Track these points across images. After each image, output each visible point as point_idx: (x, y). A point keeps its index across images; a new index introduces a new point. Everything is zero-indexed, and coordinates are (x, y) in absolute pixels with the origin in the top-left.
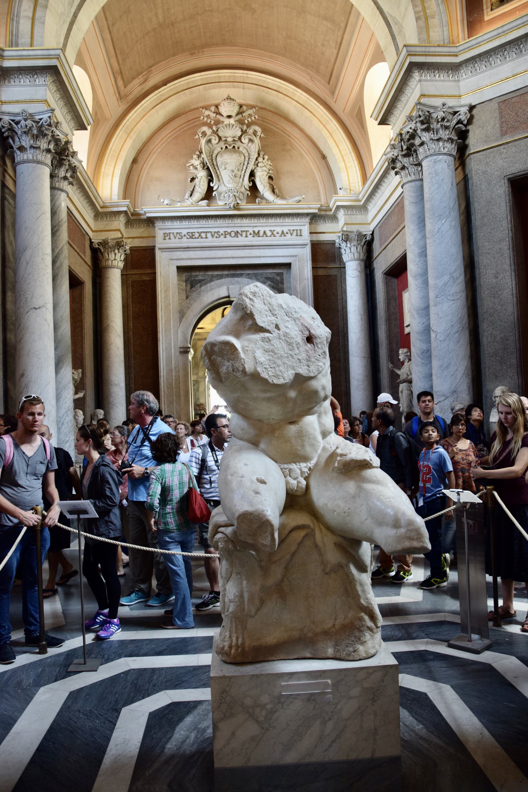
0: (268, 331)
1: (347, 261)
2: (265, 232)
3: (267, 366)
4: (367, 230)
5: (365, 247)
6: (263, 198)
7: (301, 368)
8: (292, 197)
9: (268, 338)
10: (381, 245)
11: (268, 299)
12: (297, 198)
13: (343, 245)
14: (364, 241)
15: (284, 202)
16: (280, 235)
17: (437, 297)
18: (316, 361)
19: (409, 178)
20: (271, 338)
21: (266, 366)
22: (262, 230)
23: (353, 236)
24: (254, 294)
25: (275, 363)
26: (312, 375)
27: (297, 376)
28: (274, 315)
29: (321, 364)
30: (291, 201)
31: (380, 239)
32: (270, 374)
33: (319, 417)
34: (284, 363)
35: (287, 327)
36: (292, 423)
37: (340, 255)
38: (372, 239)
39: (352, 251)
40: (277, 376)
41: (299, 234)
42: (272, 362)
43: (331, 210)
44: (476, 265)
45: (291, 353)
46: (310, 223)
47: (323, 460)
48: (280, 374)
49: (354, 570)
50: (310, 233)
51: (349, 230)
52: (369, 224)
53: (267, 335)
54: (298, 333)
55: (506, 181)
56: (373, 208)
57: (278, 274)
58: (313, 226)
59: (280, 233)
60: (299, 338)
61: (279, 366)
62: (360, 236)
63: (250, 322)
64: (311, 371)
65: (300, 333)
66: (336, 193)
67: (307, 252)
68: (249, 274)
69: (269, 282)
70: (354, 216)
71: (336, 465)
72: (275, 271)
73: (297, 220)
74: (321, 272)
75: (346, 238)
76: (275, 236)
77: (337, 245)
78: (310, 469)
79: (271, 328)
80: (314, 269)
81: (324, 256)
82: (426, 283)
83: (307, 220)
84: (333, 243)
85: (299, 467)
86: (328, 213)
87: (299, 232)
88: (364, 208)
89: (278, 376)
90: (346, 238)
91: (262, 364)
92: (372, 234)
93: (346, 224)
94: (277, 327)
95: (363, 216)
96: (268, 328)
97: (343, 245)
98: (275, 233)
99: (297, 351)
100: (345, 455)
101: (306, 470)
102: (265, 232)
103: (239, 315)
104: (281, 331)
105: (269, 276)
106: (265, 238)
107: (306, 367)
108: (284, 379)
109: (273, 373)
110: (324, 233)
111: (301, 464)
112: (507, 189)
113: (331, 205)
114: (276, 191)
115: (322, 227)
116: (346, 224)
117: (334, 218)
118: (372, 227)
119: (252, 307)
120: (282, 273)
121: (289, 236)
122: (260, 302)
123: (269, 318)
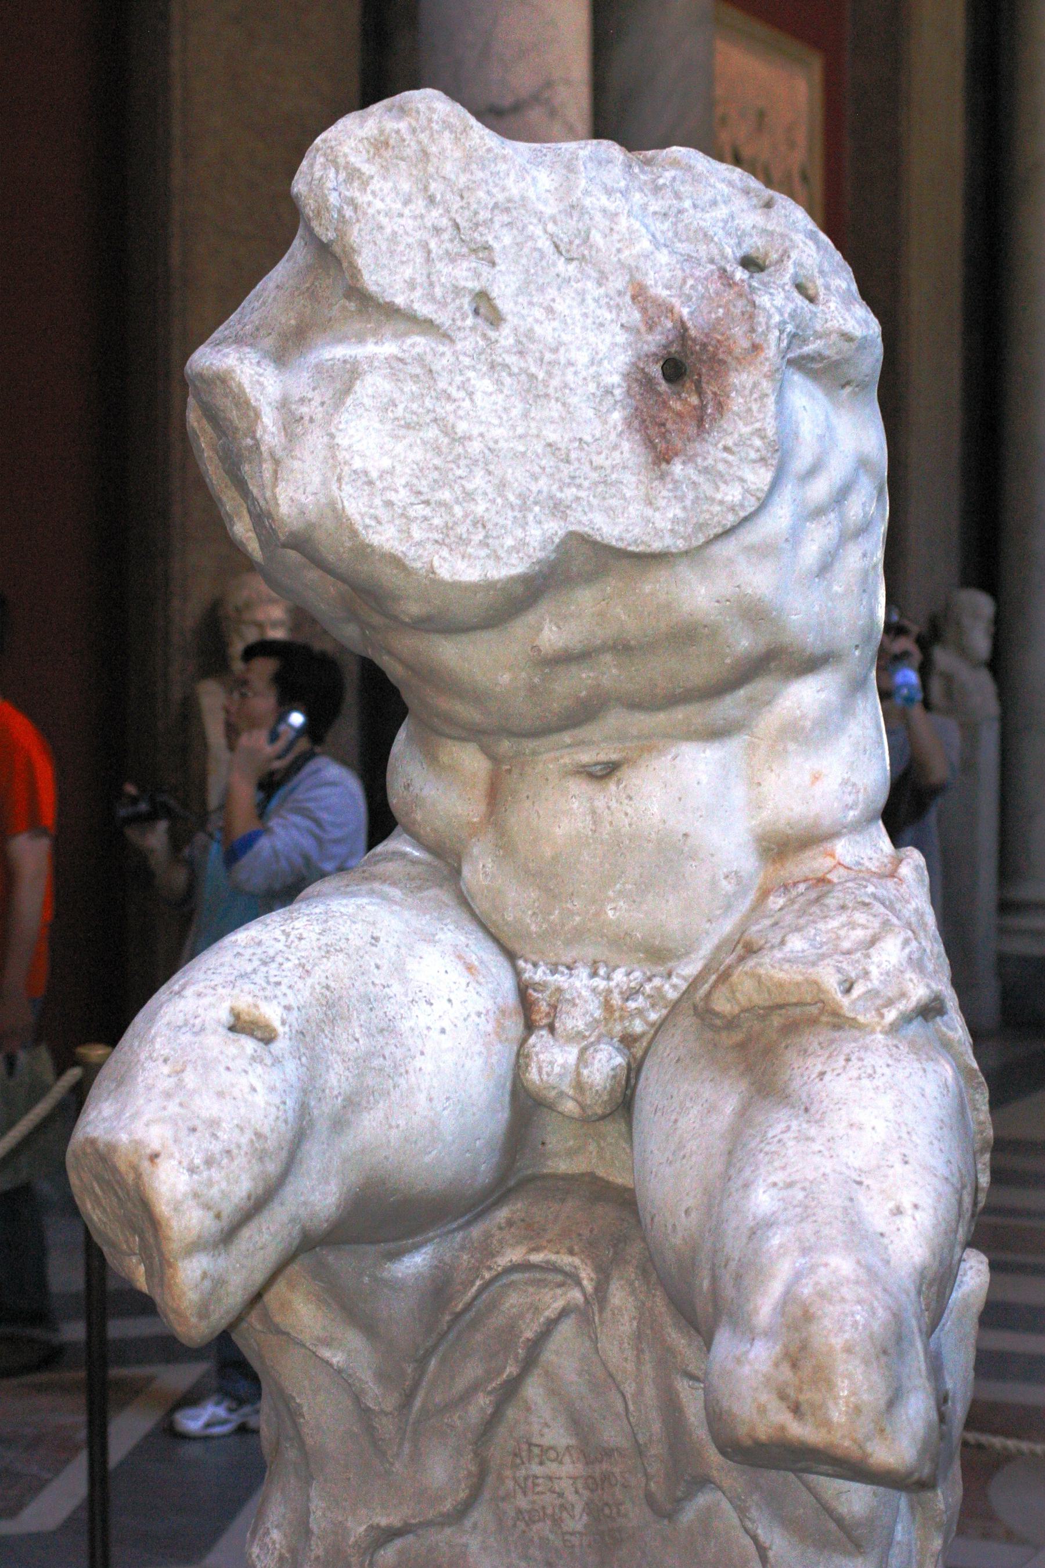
0: (427, 326)
3: (401, 497)
11: (449, 169)
18: (701, 479)
32: (417, 534)
53: (419, 343)
61: (469, 496)
65: (622, 338)
85: (600, 984)
91: (370, 483)
94: (485, 307)
96: (424, 309)
104: (506, 329)
119: (348, 212)
122: (405, 186)
123: (442, 267)
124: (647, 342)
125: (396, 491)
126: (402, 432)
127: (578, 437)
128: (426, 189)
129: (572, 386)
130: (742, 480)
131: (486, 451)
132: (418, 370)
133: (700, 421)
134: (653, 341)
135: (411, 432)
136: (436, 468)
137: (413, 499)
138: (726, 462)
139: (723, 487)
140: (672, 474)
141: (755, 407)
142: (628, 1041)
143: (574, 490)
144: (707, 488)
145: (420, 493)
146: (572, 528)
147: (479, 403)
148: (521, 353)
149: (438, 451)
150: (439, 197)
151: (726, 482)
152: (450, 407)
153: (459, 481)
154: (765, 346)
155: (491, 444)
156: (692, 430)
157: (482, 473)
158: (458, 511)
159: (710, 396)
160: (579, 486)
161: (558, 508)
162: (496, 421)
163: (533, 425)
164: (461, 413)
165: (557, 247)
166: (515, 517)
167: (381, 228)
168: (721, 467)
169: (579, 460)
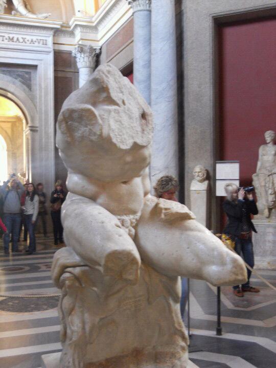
0: (117, 104)
1: (81, 68)
2: (18, 39)
3: (116, 133)
4: (97, 46)
5: (95, 58)
6: (17, 11)
7: (138, 138)
8: (40, 13)
9: (118, 110)
10: (107, 57)
12: (45, 15)
13: (78, 55)
14: (94, 53)
15: (34, 16)
16: (29, 42)
17: (157, 99)
19: (139, 8)
22: (16, 37)
23: (86, 49)
24: (109, 72)
25: (121, 131)
26: (145, 144)
28: (122, 92)
29: (150, 137)
30: (40, 16)
31: (107, 53)
33: (143, 180)
34: (127, 133)
35: (130, 104)
36: (125, 183)
37: (75, 63)
38: (100, 53)
39: (85, 60)
41: (45, 43)
43: (70, 27)
44: (185, 77)
46: (54, 36)
47: (147, 215)
48: (124, 141)
49: (171, 302)
50: (54, 43)
51: (83, 44)
52: (98, 41)
53: (116, 107)
54: (137, 110)
55: (211, 18)
56: (102, 29)
57: (27, 73)
58: (56, 38)
59: (30, 40)
60: (136, 114)
61: (124, 134)
62: (92, 49)
63: (104, 95)
66: (74, 14)
67: (50, 58)
68: (4, 71)
69: (20, 79)
70: (87, 34)
71: (163, 216)
72: (24, 70)
73: (44, 32)
74: (60, 75)
75: (82, 50)
76: (26, 43)
77: (73, 55)
78: (136, 220)
79: (120, 102)
80: (56, 71)
81: (63, 62)
82: (149, 88)
83: (52, 33)
84: (70, 53)
86: (68, 29)
87: (45, 41)
88: (95, 28)
90: (82, 50)
92: (100, 49)
93: (82, 39)
95: (95, 35)
97: (78, 55)
98: (26, 40)
100: (169, 209)
101: (134, 221)
102: (18, 39)
103: (94, 89)
105: (20, 74)
106: (17, 43)
107: (141, 138)
110: (64, 44)
111: (130, 216)
112: (211, 24)
113: (70, 23)
114: (28, 7)
115: (63, 39)
116: (82, 39)
117: (72, 33)
118: (100, 43)
120: (30, 72)
121: (36, 44)
128: (115, 80)
133: (147, 125)
134: (141, 112)
142: (133, 227)
146: (136, 141)
149: (120, 125)
161: (133, 137)
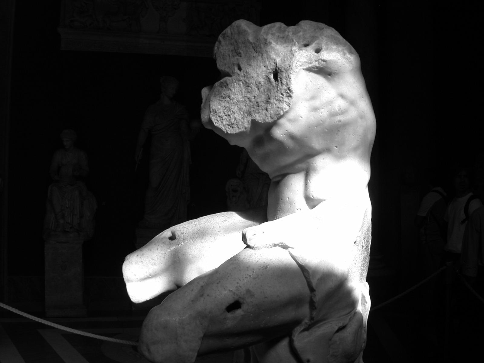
18: (276, 102)
20: (228, 82)
21: (220, 114)
26: (269, 120)
27: (254, 123)
40: (231, 125)
42: (228, 109)
45: (249, 96)
64: (269, 115)
89: (233, 124)
91: (216, 112)
99: (256, 92)
104: (242, 71)
107: (264, 111)
108: (238, 127)
109: (227, 121)
124: (269, 70)
125: (220, 113)
126: (222, 99)
127: (253, 95)
129: (253, 83)
130: (286, 102)
131: (237, 102)
132: (226, 85)
135: (224, 99)
136: (228, 107)
137: (224, 115)
138: (282, 97)
139: (281, 104)
140: (271, 102)
141: (288, 82)
143: (253, 109)
144: (278, 105)
145: (225, 113)
146: (252, 118)
147: (236, 90)
148: (244, 77)
150: (233, 44)
151: (282, 103)
152: (230, 92)
153: (232, 109)
154: (291, 65)
155: (238, 100)
156: (275, 90)
157: (236, 107)
158: (232, 117)
159: (279, 81)
160: (254, 108)
162: (239, 94)
163: (246, 94)
164: (233, 93)
165: (254, 50)
166: (242, 117)
167: (221, 53)
168: (281, 99)
169: (254, 101)
